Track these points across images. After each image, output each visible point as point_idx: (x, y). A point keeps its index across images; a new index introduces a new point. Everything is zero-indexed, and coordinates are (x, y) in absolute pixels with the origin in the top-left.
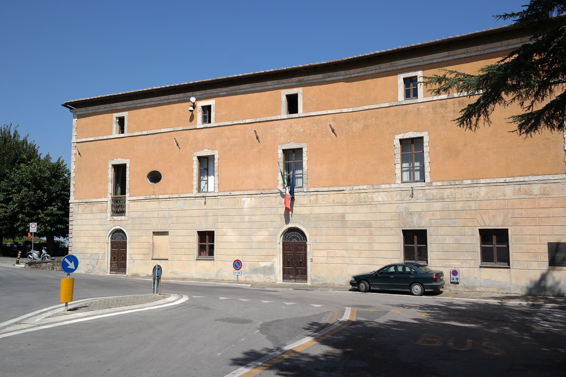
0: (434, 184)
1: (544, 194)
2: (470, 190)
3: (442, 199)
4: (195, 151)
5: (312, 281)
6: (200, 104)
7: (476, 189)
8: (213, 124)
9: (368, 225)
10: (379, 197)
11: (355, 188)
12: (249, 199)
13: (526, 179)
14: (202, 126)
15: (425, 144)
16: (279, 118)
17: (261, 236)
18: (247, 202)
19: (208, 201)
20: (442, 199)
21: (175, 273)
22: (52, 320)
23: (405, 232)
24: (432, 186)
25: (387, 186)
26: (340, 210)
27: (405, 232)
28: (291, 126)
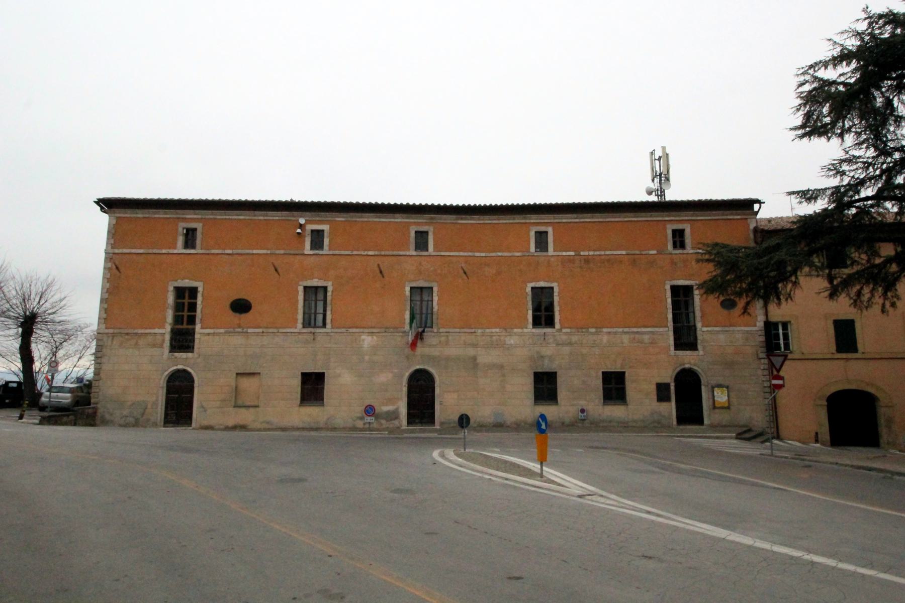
0: (564, 330)
1: (653, 343)
2: (595, 337)
3: (570, 344)
4: (302, 280)
5: (442, 424)
6: (310, 227)
7: (600, 337)
8: (326, 250)
9: (501, 367)
10: (511, 341)
11: (487, 330)
12: (370, 338)
13: (639, 330)
14: (311, 252)
15: (556, 294)
16: (408, 253)
17: (384, 377)
18: (367, 341)
19: (319, 338)
20: (570, 344)
21: (268, 423)
22: (562, 482)
23: (536, 375)
24: (558, 332)
25: (519, 330)
26: (471, 352)
27: (536, 375)
28: (420, 264)
